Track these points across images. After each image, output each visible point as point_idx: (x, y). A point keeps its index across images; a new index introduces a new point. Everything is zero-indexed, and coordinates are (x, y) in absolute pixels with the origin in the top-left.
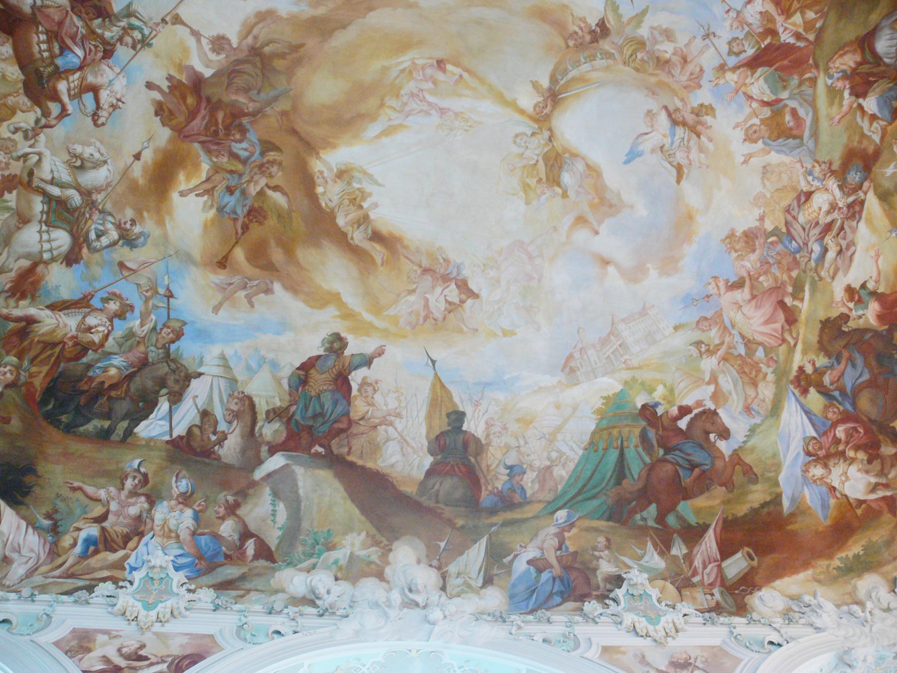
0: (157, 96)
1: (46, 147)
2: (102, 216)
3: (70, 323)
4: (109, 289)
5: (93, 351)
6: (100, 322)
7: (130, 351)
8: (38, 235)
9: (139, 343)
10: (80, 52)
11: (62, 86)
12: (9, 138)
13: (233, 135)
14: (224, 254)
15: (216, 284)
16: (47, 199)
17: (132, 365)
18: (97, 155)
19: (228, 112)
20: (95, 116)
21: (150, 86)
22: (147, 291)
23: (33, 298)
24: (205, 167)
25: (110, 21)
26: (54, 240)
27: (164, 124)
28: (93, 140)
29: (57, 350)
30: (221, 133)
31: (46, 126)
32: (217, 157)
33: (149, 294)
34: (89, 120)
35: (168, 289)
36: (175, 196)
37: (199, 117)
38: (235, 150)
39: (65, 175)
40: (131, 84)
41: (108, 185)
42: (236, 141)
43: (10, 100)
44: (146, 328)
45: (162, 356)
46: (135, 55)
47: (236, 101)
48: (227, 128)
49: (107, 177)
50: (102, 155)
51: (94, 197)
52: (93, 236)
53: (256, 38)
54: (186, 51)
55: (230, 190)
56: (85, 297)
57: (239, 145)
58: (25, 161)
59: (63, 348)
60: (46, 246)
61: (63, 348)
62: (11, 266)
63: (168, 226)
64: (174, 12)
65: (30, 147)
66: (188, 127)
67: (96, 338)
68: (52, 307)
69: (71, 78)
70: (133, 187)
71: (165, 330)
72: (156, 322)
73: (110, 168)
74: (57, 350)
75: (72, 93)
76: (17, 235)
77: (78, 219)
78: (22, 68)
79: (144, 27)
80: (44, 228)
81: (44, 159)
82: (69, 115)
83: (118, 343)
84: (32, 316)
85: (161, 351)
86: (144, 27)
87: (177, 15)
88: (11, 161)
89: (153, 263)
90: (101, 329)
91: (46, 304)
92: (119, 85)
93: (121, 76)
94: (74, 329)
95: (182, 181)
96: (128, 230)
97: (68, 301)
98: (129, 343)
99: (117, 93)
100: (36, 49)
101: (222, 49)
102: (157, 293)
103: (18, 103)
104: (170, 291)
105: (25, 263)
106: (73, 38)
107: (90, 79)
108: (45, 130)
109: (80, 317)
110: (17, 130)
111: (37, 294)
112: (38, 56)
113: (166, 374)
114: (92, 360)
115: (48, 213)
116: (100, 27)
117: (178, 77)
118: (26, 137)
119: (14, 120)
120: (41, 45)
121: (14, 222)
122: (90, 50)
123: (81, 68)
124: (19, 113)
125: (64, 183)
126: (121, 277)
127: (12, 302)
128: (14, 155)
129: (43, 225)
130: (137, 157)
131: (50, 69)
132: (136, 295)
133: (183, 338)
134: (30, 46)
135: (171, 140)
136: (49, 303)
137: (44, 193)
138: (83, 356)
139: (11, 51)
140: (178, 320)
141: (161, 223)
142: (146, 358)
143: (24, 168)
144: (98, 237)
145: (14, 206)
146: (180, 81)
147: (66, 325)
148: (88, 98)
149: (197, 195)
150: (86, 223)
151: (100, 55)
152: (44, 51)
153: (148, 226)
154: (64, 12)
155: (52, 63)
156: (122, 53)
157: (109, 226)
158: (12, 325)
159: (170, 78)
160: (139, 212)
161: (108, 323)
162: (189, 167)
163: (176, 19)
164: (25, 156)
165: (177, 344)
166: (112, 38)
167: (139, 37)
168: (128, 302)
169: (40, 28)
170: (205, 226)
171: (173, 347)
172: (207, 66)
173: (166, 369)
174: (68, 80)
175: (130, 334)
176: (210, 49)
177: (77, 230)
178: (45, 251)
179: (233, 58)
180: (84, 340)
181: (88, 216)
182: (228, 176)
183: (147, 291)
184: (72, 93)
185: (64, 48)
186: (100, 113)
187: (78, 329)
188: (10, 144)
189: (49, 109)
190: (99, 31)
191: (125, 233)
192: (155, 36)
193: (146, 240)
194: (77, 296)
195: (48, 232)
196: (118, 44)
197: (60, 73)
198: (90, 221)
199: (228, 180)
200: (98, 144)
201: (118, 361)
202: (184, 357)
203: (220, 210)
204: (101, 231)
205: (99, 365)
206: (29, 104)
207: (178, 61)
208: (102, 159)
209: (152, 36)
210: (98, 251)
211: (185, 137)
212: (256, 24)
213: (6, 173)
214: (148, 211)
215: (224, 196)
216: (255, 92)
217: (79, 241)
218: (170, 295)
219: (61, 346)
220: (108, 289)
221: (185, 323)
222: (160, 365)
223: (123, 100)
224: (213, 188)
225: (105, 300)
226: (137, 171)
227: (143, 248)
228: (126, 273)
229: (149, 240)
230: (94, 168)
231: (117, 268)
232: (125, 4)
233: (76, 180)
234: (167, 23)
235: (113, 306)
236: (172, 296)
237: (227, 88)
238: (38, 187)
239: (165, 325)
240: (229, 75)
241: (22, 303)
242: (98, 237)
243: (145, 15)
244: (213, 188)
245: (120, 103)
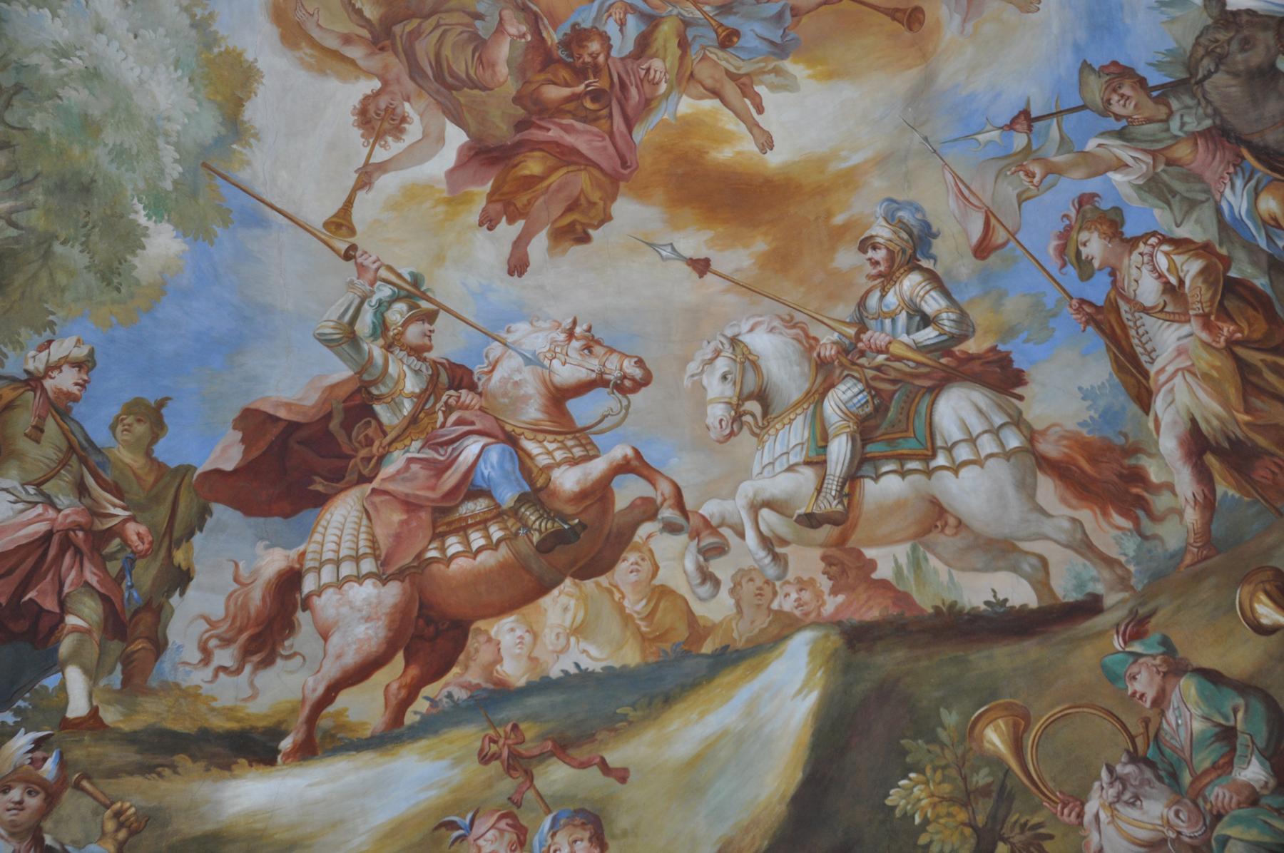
0: (539, 246)
1: (732, 495)
2: (872, 324)
3: (1169, 343)
4: (1053, 264)
5: (1228, 266)
6: (1146, 270)
7: (1199, 179)
8: (964, 472)
9: (1170, 163)
10: (472, 448)
11: (568, 480)
12: (732, 592)
13: (594, 56)
14: (888, 19)
15: (964, 21)
16: (867, 469)
17: (1238, 162)
18: (722, 365)
19: (542, 77)
20: (624, 387)
21: (518, 266)
22: (1031, 175)
23: (1135, 450)
24: (686, 105)
25: (374, 383)
26: (965, 427)
27: (607, 218)
28: (687, 382)
29: (1254, 357)
30: (596, 83)
31: (680, 504)
32: (656, 84)
33: (1037, 170)
34: (637, 399)
35: (1011, 126)
36: (774, 160)
37: (569, 139)
38: (630, 47)
39: (793, 435)
40: (523, 309)
41: (791, 323)
42: (608, 47)
43: (635, 605)
44: (1126, 154)
45: (1188, 100)
46: (448, 311)
47: (509, 63)
48: (581, 73)
49: (772, 330)
50: (718, 354)
51: (829, 352)
52: (928, 335)
53: (347, 40)
54: (412, 193)
55: (728, 39)
56: (1091, 320)
57: (616, 39)
58: (784, 542)
59: (1244, 343)
60: (988, 445)
61: (1244, 343)
62: (1066, 524)
63: (856, 159)
64: (325, 234)
65: (742, 535)
66: (604, 164)
67: (1192, 268)
68: (1144, 398)
69: (543, 460)
70: (781, 260)
71: (1117, 108)
72: (1102, 134)
73: (745, 327)
74: (1254, 357)
75: (578, 452)
76: (977, 525)
77: (894, 382)
78: (543, 588)
79: (374, 300)
80: (941, 460)
81: (766, 495)
82: (637, 452)
83: (1187, 214)
84: (1182, 443)
85: (1175, 104)
86: (374, 300)
87: (327, 225)
88: (790, 576)
89: (955, 176)
90: (1162, 262)
91: (1140, 412)
92: (535, 339)
93: (510, 339)
94: (1186, 329)
95: (735, 148)
96: (891, 253)
97: (1115, 360)
98: (1177, 185)
99: (553, 342)
100: (487, 559)
101: (390, 111)
102: (1027, 150)
103: (636, 584)
104: (1014, 121)
105: (1047, 489)
106: (440, 469)
107: (533, 411)
108: (689, 503)
109: (1148, 320)
110: (707, 577)
111: (1120, 441)
112: (504, 551)
113: (1236, 75)
114: (1255, 264)
115: (902, 458)
116: (395, 406)
117: (480, 203)
118: (721, 550)
119: (683, 589)
120: (475, 546)
121: (946, 541)
122: (459, 422)
123: (511, 440)
124: (661, 578)
125: (813, 433)
126: (1012, 244)
127: (1161, 502)
128: (771, 571)
129: (933, 464)
130: (701, 266)
131: (531, 516)
132: (1047, 197)
133: (1122, 62)
134: (481, 577)
135: (641, 194)
136: (1134, 408)
137: (852, 478)
138: (1252, 289)
139: (508, 621)
140: (1082, 84)
141: (850, 179)
142: (1205, 134)
143: (802, 542)
144: (926, 321)
145: (907, 547)
146: (491, 198)
147: (1180, 352)
148: (583, 410)
149: (760, 110)
150: (900, 359)
151: (466, 397)
152: (488, 537)
153: (866, 208)
154: (377, 499)
155: (514, 512)
156: (448, 343)
157: (892, 299)
158: (1224, 489)
159: (488, 222)
160: (838, 235)
161: (1142, 248)
162: (696, 142)
163: (339, 226)
164: (767, 542)
165: (1143, 71)
166: (417, 372)
167: (401, 306)
168: (1073, 213)
169: (432, 554)
170: (830, 76)
171: (1155, 78)
172: (441, 140)
173: (1220, 78)
174: (549, 468)
175: (1153, 187)
176: (398, 139)
177: (925, 376)
178: (1002, 445)
179: (410, 85)
180: (1207, 296)
181: (881, 358)
182: (694, 53)
183: (1031, 175)
184: (578, 452)
185: (470, 488)
186: (613, 376)
187: (1181, 317)
188: (748, 589)
189: (632, 506)
190: (407, 407)
191: (898, 259)
192: (390, 269)
193: (900, 205)
194: (1093, 337)
195: (949, 449)
196: (431, 355)
197: (537, 491)
198: (895, 349)
199: (704, 48)
200: (693, 367)
201: (1236, 200)
202: (1173, 45)
203: (780, 50)
204: (910, 317)
205: (1263, 243)
206: (632, 557)
207: (441, 209)
208: (728, 352)
209: (393, 278)
210: (963, 314)
211: (624, 164)
212: (314, 43)
213: (825, 584)
214: (829, 215)
215: (742, 48)
216: (478, 23)
217: (950, 366)
218: (1025, 119)
219: (1241, 351)
220: (1054, 271)
221: (1085, 67)
222: (1214, 96)
223: (567, 323)
224: (733, 77)
225: (1085, 268)
226: (738, 258)
227: (927, 206)
228: (1000, 236)
229: (900, 197)
230: (755, 366)
231: (992, 258)
232: (325, 350)
233: (798, 404)
234: (353, 247)
235: (1095, 246)
236: (1025, 113)
237: (485, 89)
238: (840, 495)
239: (1105, 111)
240: (449, 90)
241: (1155, 476)
242: (926, 321)
243: (342, 303)
244: (733, 77)
245: (578, 330)
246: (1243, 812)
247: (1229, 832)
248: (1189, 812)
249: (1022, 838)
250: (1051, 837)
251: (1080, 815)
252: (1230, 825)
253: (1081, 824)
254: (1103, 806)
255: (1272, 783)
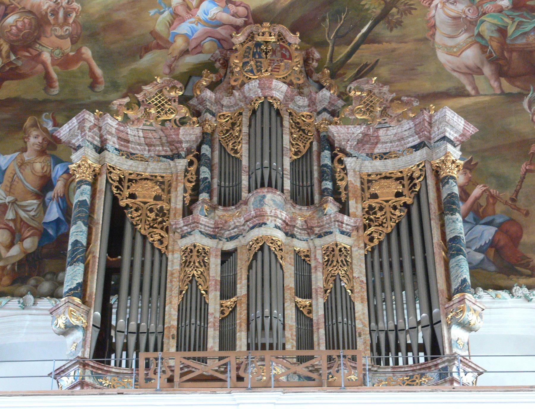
246: (495, 14)
247: (486, 19)
248: (474, 10)
249: (404, 8)
250: (415, 9)
251: (430, 4)
252: (487, 17)
253: (429, 7)
254: (440, 2)
255: (510, 7)
